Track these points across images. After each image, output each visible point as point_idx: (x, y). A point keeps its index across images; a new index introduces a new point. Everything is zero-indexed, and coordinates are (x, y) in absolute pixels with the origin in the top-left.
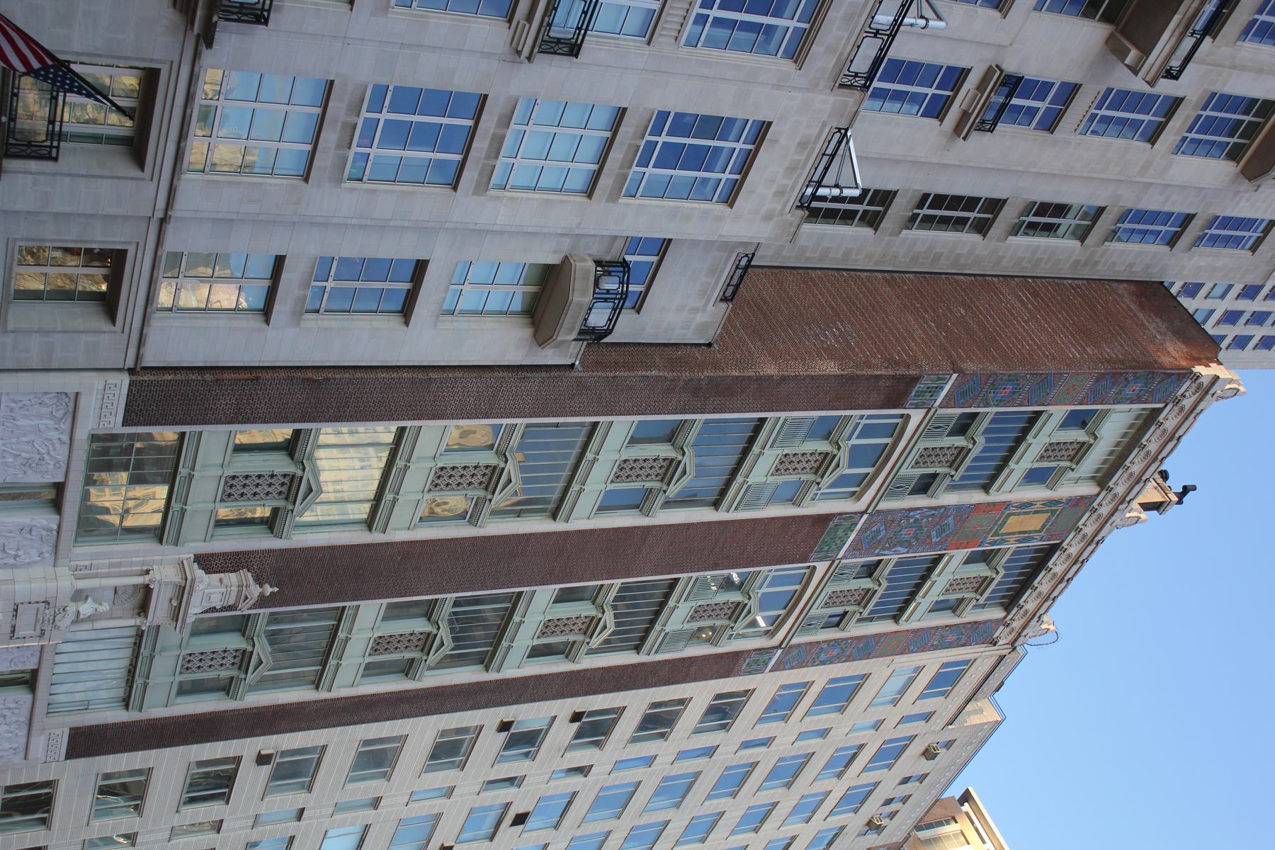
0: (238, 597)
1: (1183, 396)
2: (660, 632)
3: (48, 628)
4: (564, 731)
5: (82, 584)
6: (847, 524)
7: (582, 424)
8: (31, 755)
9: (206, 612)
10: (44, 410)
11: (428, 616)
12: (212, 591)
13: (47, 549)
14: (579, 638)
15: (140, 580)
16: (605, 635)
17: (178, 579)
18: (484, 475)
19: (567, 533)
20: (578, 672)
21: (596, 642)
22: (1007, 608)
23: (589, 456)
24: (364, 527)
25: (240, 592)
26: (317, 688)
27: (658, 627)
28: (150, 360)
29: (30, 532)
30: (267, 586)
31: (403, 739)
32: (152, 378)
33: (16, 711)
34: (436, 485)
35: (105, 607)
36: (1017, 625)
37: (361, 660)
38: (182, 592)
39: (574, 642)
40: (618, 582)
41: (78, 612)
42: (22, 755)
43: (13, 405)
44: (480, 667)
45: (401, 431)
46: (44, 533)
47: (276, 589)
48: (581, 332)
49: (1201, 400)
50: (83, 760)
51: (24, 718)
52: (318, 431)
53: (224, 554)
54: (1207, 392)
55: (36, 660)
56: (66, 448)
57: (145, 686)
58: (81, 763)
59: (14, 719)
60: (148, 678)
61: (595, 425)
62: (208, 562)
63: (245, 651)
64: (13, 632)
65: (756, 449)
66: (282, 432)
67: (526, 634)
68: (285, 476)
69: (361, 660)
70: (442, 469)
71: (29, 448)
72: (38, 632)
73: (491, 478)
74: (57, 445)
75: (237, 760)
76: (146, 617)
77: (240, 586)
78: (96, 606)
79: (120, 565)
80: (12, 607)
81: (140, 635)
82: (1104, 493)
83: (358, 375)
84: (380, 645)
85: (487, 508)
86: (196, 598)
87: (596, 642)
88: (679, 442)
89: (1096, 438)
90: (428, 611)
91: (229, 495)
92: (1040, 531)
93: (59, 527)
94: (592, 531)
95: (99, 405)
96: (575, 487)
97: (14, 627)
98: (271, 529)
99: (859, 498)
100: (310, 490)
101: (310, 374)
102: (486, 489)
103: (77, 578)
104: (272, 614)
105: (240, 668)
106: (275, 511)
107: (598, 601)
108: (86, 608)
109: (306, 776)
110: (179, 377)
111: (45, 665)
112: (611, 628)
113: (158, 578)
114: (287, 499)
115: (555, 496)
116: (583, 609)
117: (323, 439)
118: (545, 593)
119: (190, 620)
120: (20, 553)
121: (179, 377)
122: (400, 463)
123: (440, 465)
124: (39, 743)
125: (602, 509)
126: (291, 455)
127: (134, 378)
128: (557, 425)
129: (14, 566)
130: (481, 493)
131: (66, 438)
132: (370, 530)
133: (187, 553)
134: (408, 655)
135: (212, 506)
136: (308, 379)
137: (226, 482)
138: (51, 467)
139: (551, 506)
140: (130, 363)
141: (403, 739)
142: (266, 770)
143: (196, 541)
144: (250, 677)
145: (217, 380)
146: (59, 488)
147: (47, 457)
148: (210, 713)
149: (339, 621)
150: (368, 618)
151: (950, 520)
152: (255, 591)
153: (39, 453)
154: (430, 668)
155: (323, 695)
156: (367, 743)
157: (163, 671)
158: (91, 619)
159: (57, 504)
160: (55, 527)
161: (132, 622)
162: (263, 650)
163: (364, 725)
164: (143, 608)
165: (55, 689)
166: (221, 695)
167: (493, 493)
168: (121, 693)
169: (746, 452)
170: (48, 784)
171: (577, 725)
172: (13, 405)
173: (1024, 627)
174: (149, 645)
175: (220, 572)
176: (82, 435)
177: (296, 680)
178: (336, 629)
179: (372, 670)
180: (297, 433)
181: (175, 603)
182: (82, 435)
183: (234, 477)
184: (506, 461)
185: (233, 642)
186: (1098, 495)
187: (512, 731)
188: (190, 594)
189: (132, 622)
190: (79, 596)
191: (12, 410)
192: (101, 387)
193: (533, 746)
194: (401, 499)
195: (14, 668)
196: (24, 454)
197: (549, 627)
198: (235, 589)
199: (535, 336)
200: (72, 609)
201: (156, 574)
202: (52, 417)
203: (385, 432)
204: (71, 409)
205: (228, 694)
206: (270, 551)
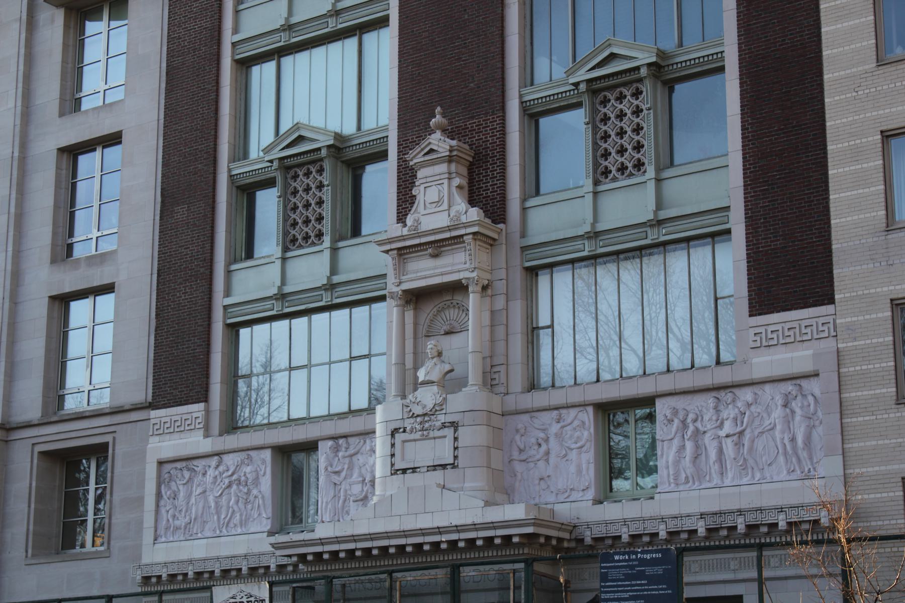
0: (433, 163)
3: (442, 418)
8: (808, 368)
46: (340, 454)
47: (439, 109)
50: (836, 272)
51: (708, 401)
56: (226, 458)
64: (444, 466)
72: (449, 432)
97: (435, 467)
111: (576, 396)
122: (283, 40)
131: (214, 461)
138: (248, 469)
153: (230, 486)
204: (184, 464)
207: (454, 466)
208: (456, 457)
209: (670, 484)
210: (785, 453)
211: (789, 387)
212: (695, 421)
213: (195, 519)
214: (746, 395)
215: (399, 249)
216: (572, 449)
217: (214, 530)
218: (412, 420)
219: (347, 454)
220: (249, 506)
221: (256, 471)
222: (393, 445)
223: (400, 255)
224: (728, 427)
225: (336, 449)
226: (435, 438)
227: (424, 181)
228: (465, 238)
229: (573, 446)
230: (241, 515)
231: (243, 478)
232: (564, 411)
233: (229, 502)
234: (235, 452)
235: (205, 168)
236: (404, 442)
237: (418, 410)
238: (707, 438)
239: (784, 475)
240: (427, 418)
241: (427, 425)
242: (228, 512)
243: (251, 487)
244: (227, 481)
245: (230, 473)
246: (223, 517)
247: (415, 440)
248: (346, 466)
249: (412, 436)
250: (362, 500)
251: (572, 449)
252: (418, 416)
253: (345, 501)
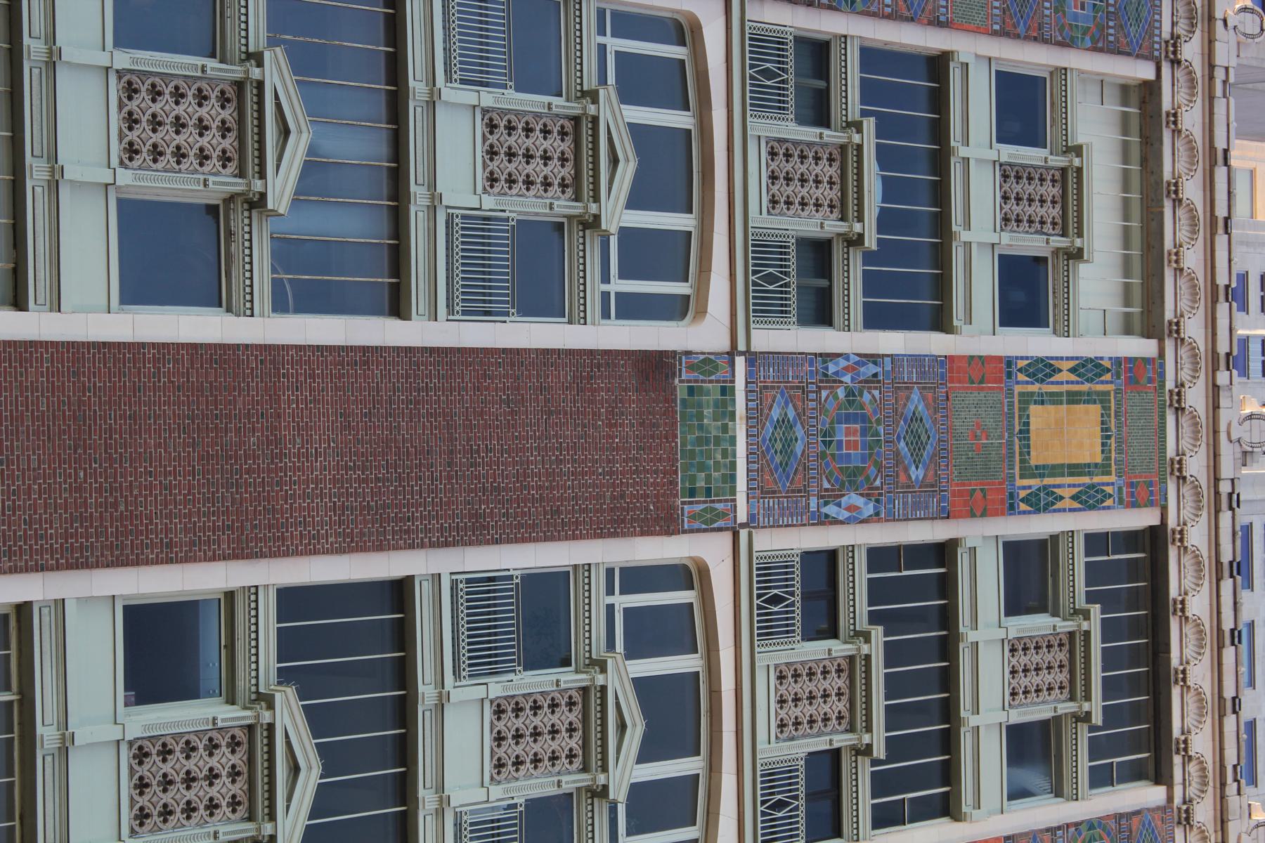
1: (1175, 38)
2: (440, 813)
6: (713, 388)
22: (1160, 775)
27: (426, 797)
36: (1204, 813)
49: (1210, 42)
54: (1211, 18)
65: (417, 86)
82: (1169, 345)
88: (234, 45)
89: (1078, 150)
92: (1104, 469)
99: (702, 312)
107: (242, 683)
151: (916, 403)
169: (396, 107)
173: (1223, 822)
186: (1162, 354)
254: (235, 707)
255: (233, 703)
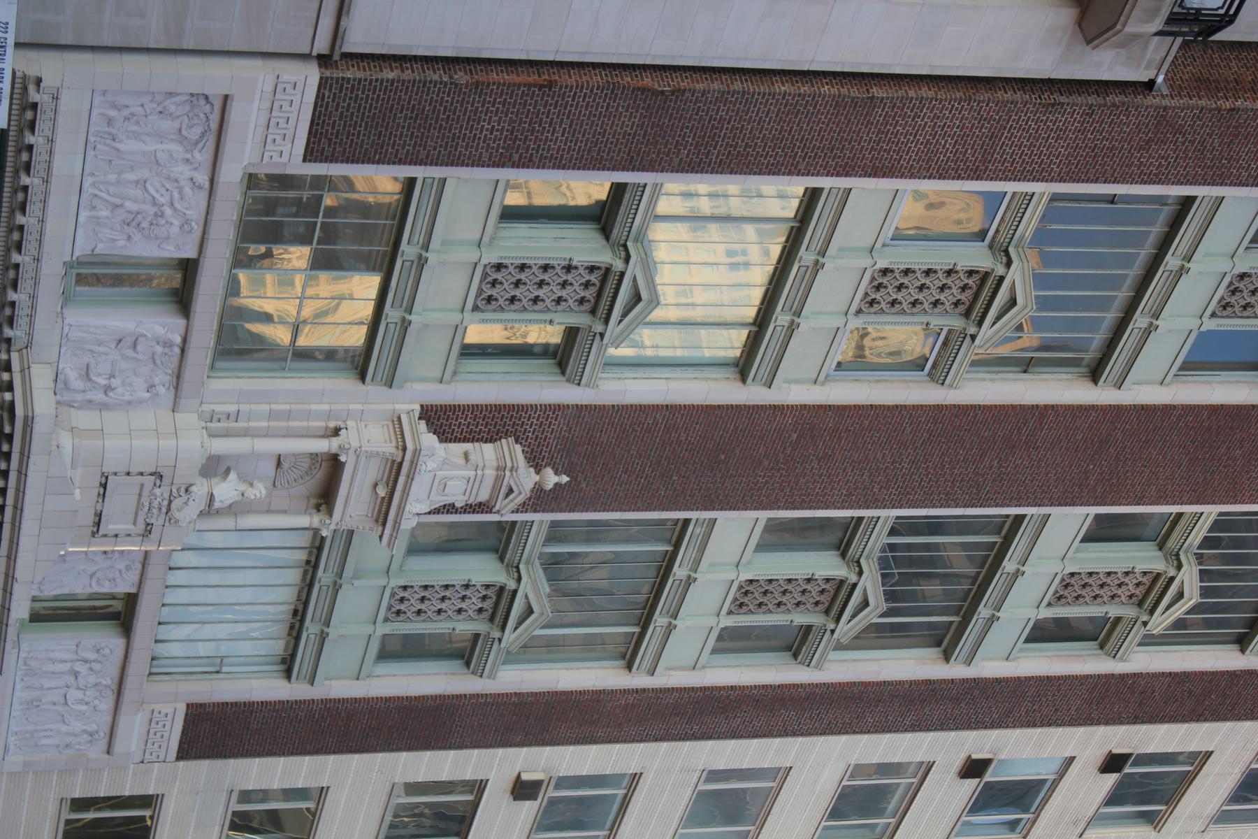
3: (157, 521)
4: (1087, 789)
5: (220, 446)
7: (1161, 200)
8: (118, 747)
9: (437, 511)
10: (167, 125)
11: (843, 548)
12: (452, 474)
13: (162, 378)
14: (1129, 612)
15: (323, 446)
16: (1179, 611)
17: (390, 448)
18: (964, 288)
19: (1117, 412)
20: (1123, 677)
21: (1160, 622)
23: (1171, 261)
24: (731, 373)
25: (499, 479)
26: (629, 667)
28: (359, 39)
29: (135, 345)
30: (549, 472)
31: (781, 775)
32: (360, 75)
33: (97, 666)
34: (872, 303)
35: (258, 491)
37: (712, 621)
38: (396, 472)
39: (1118, 620)
40: (1211, 511)
41: (212, 497)
42: (102, 745)
43: (113, 113)
44: (933, 653)
45: (812, 196)
46: (159, 349)
47: (565, 479)
48: (1172, 19)
51: (109, 680)
52: (657, 188)
53: (474, 408)
55: (134, 577)
56: (204, 195)
57: (323, 637)
58: (204, 767)
59: (92, 679)
60: (327, 624)
61: (1187, 202)
62: (446, 422)
63: (502, 589)
64: (98, 524)
66: (588, 188)
67: (1025, 595)
68: (592, 269)
69: (712, 621)
70: (885, 272)
71: (138, 193)
72: (141, 526)
73: (977, 296)
74: (187, 190)
75: (478, 787)
76: (330, 513)
77: (501, 469)
78: (243, 487)
79: (288, 416)
80: (98, 479)
81: (318, 546)
83: (738, 86)
84: (750, 595)
85: (967, 353)
86: (420, 487)
87: (1160, 622)
90: (843, 539)
91: (490, 299)
93: (185, 340)
94: (1168, 409)
95: (264, 121)
96: (1140, 320)
98: (562, 366)
100: (637, 298)
101: (647, 81)
102: (967, 315)
103: (212, 435)
104: (554, 524)
105: (492, 619)
106: (571, 334)
107: (1171, 543)
108: (226, 490)
109: (602, 829)
110: (407, 75)
111: (148, 587)
112: (1193, 597)
113: (355, 444)
114: (593, 312)
115: (1099, 338)
116: (1141, 558)
117: (663, 207)
118: (1068, 521)
119: (408, 524)
120: (115, 382)
121: (407, 75)
122: (806, 256)
123: (882, 264)
124: (133, 728)
125: (1190, 366)
126: (606, 232)
127: (328, 73)
128: (1112, 199)
129: (103, 407)
130: (957, 323)
131: (203, 178)
132: (744, 379)
133: (407, 400)
134: (800, 619)
135: (455, 318)
136: (644, 90)
137: (485, 275)
138: (175, 230)
139: (1091, 355)
140: (322, 46)
141: (781, 775)
142: (529, 809)
143: (427, 380)
144: (510, 636)
145: (477, 84)
146: (189, 268)
147: (168, 211)
148: (435, 698)
149: (677, 546)
150: (731, 545)
152: (527, 479)
153: (154, 203)
154: (839, 647)
155: (638, 680)
156: (714, 776)
157: (356, 614)
158: (233, 510)
159: (182, 299)
160: (178, 340)
161: (304, 521)
162: (536, 590)
163: (710, 743)
164: (325, 497)
165: (165, 632)
166: (457, 665)
167: (980, 324)
168: (278, 647)
170: (147, 801)
171: (1112, 778)
172: (113, 113)
174: (334, 566)
175: (465, 440)
176: (232, 173)
177: (590, 649)
178: (670, 559)
179: (732, 641)
180: (618, 191)
181: (382, 492)
182: (232, 173)
183: (499, 267)
184: (1009, 264)
185: (481, 570)
187: (988, 777)
188: (410, 477)
189: (304, 521)
190: (214, 467)
191: (110, 122)
192: (269, 88)
193: (1026, 810)
194: (804, 324)
195: (96, 589)
196: (128, 204)
197: (1070, 587)
198: (491, 473)
199: (1080, 23)
200: (201, 489)
201: (350, 437)
202: (180, 137)
203: (779, 196)
204: (214, 126)
205: (468, 664)
206: (558, 408)
207: (93, 534)
208: (105, 536)
209: (29, 652)
210: (36, 731)
211: (103, 734)
212: (91, 669)
213: (118, 150)
214: (106, 705)
215: (401, 464)
216: (91, 577)
217: (92, 174)
218: (166, 496)
219: (157, 357)
220: (118, 227)
221: (168, 238)
222: (142, 474)
223: (393, 461)
224: (74, 695)
225: (168, 344)
226: (136, 514)
227: (478, 479)
228: (380, 528)
229: (94, 580)
230: (107, 218)
231: (162, 222)
232: (138, 572)
233: (130, 199)
234: (207, 213)
235: (676, 161)
236: (142, 485)
237: (176, 504)
238: (71, 679)
239: (15, 729)
240: (164, 510)
241: (155, 511)
242: (119, 197)
243: (146, 232)
244: (162, 200)
245: (177, 205)
246: (112, 189)
247: (140, 495)
248: (140, 357)
249: (146, 493)
250: (87, 375)
251: (91, 577)
252: (170, 502)
253: (92, 351)
254: (1160, 553)
255: (1160, 549)
